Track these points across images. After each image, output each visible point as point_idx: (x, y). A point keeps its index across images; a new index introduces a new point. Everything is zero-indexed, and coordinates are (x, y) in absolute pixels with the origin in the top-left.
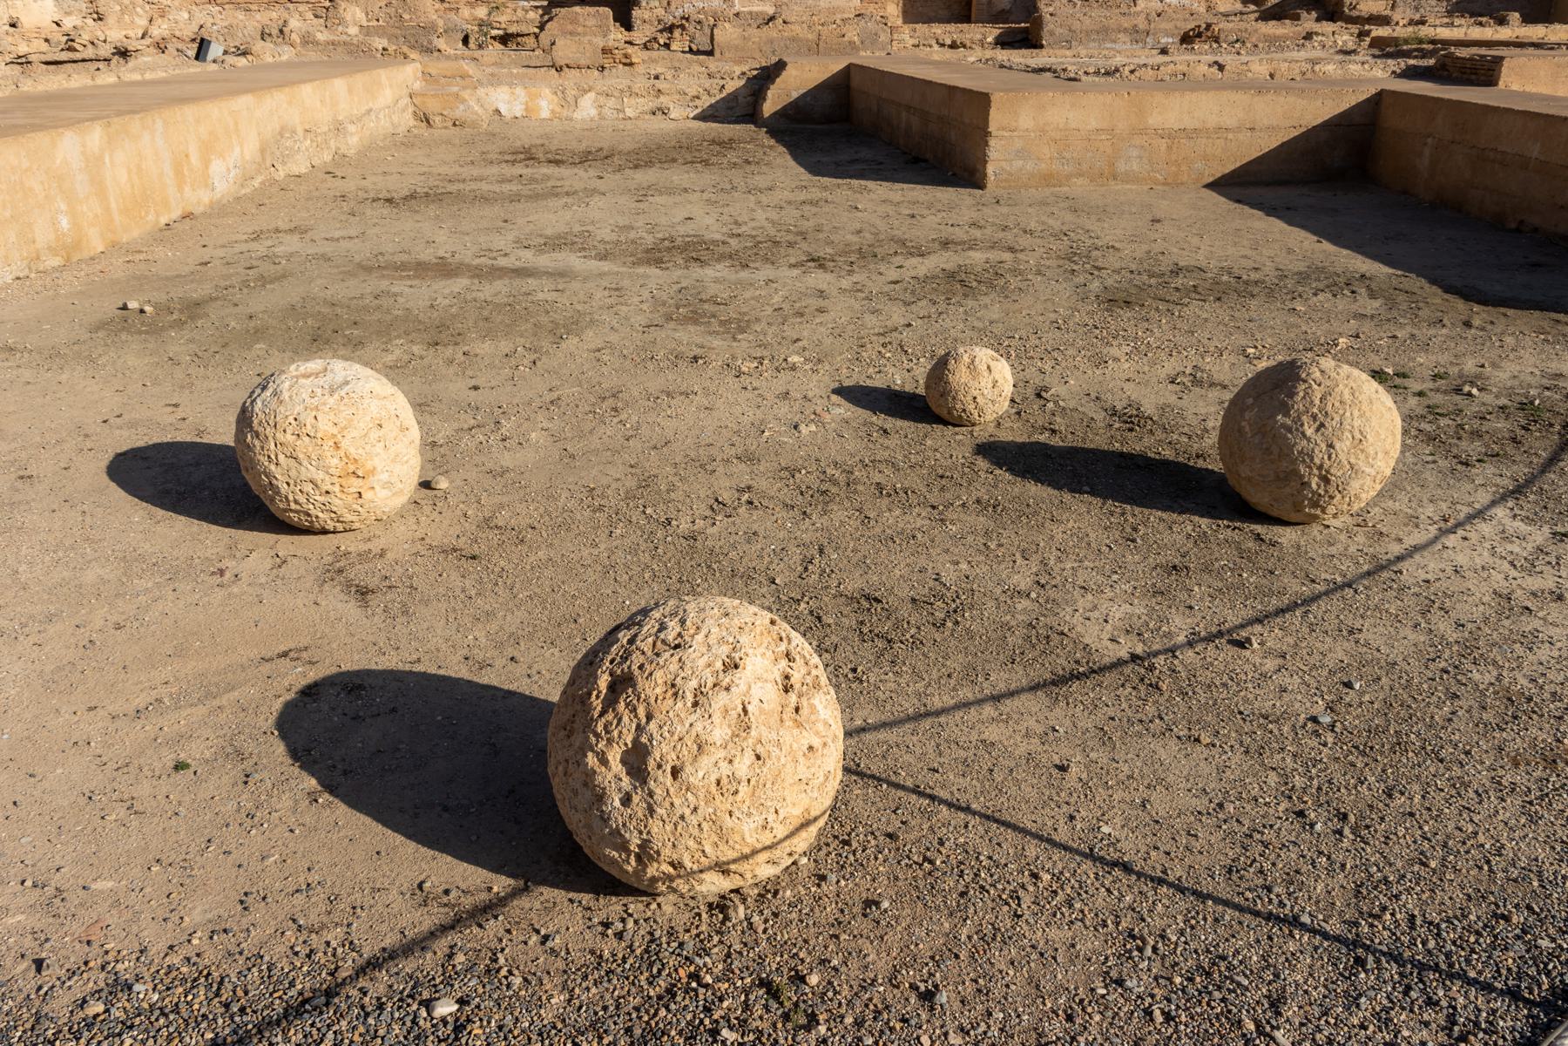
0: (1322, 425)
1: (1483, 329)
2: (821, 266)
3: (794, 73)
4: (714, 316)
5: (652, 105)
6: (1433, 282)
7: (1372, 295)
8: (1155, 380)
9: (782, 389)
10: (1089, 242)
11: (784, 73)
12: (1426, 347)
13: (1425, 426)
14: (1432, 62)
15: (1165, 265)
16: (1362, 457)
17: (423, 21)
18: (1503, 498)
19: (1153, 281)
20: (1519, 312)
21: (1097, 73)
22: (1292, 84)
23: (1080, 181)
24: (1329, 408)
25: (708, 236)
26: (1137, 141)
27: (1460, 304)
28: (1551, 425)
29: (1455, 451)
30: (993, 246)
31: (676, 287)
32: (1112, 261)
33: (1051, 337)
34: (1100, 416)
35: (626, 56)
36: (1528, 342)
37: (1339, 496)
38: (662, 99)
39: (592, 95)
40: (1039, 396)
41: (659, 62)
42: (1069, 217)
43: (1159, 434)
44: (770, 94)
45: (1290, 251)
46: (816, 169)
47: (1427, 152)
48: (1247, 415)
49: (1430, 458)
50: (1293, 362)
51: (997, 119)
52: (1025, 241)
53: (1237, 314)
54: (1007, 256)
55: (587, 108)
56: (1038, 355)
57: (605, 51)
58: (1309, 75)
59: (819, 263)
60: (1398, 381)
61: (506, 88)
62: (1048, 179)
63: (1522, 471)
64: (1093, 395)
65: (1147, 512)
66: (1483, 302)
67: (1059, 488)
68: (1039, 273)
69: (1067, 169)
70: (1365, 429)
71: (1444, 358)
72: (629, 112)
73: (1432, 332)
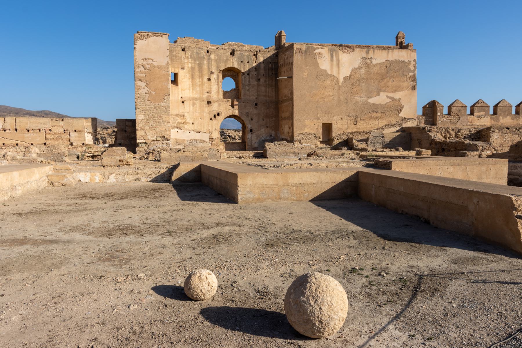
0: (316, 300)
1: (389, 250)
2: (170, 235)
3: (182, 167)
4: (118, 258)
5: (135, 177)
6: (375, 233)
7: (355, 239)
8: (276, 276)
9: (131, 289)
10: (266, 222)
11: (179, 167)
12: (370, 258)
13: (368, 290)
14: (373, 162)
15: (290, 229)
16: (333, 312)
17: (60, 152)
18: (392, 321)
19: (283, 236)
20: (400, 243)
21: (274, 167)
22: (333, 169)
23: (269, 200)
24: (318, 293)
25: (134, 224)
26: (286, 187)
27: (382, 241)
28: (409, 287)
29: (377, 300)
30: (234, 224)
31: (110, 246)
32: (273, 229)
33: (242, 260)
34: (252, 293)
35: (127, 162)
36: (403, 254)
37: (327, 328)
38: (139, 175)
39: (114, 175)
40: (232, 285)
41: (140, 164)
42: (263, 213)
43: (273, 300)
44: (174, 173)
45: (331, 223)
46: (183, 198)
47: (373, 189)
48: (292, 296)
49: (368, 304)
50: (306, 275)
51: (240, 182)
52: (245, 222)
53: (309, 248)
54: (237, 228)
55: (112, 179)
56: (235, 268)
57: (120, 161)
58: (338, 167)
59: (169, 233)
60: (360, 272)
61: (83, 173)
62: (259, 200)
63: (399, 307)
64: (252, 284)
65: (259, 337)
66: (389, 240)
67: (227, 329)
68: (246, 234)
69: (265, 197)
70: (334, 300)
71: (376, 262)
72: (127, 180)
73: (373, 252)
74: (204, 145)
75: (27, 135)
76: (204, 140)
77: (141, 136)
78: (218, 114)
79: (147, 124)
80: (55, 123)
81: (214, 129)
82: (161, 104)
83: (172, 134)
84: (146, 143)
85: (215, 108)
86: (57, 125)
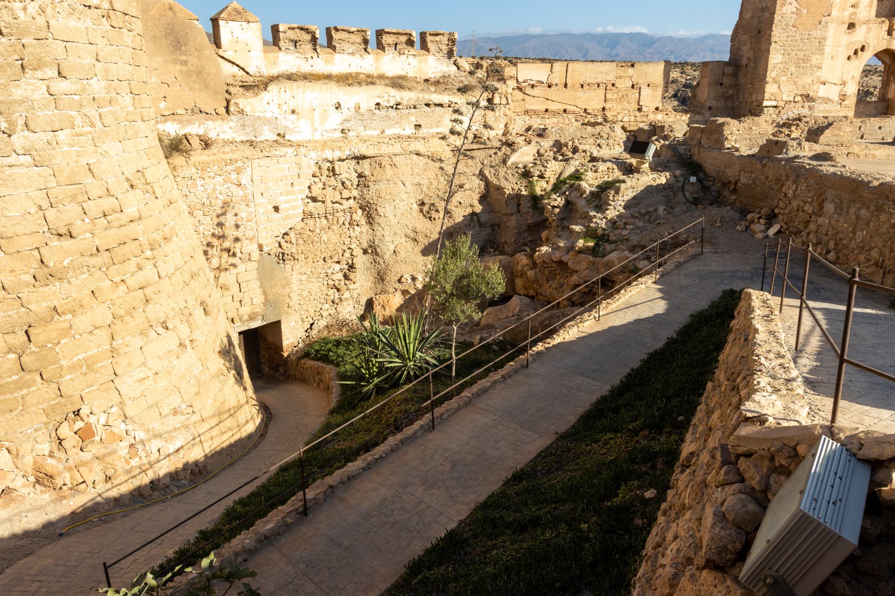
74: (829, 107)
75: (580, 93)
76: (830, 97)
77: (772, 94)
78: (863, 49)
79: (784, 71)
80: (621, 72)
81: (851, 76)
82: (814, 33)
83: (820, 91)
84: (776, 107)
85: (860, 36)
86: (624, 75)
